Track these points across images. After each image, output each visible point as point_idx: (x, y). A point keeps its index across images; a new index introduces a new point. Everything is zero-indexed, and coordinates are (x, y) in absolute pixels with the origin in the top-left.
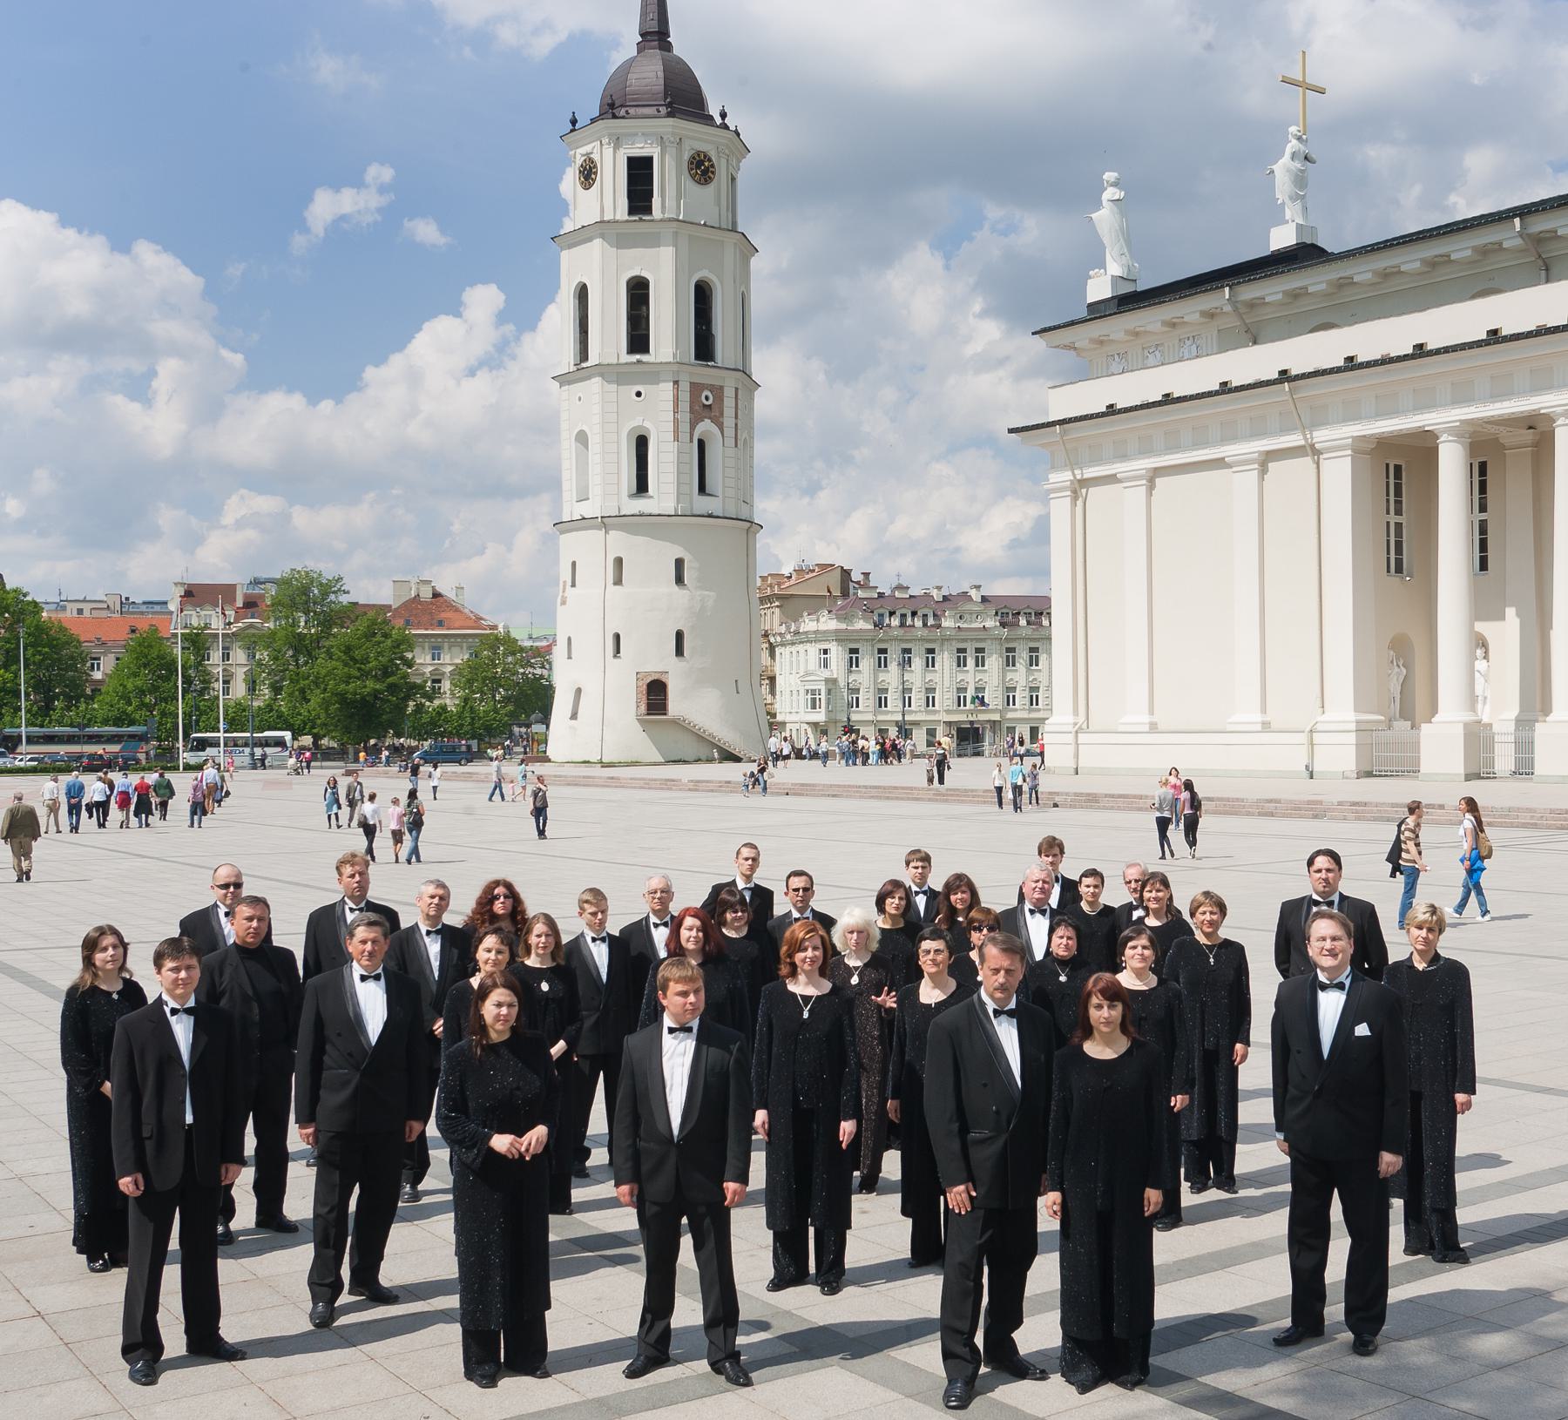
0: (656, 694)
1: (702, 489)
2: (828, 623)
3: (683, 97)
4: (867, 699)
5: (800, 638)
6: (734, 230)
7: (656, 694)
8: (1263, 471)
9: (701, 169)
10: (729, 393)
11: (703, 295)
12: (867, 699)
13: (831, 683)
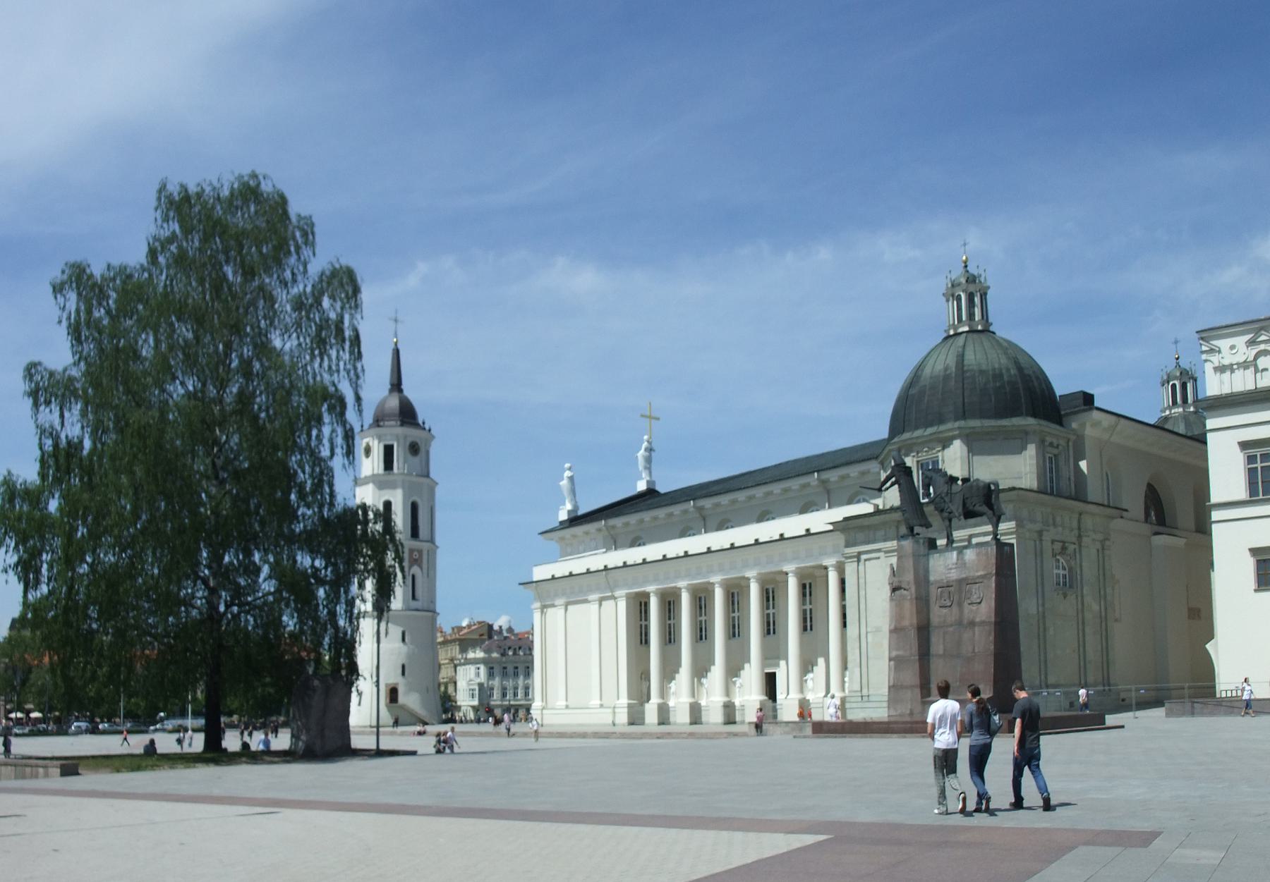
0: (393, 693)
1: (414, 597)
2: (480, 654)
3: (407, 414)
4: (497, 694)
5: (468, 662)
6: (428, 476)
7: (393, 693)
8: (600, 605)
9: (414, 449)
10: (425, 553)
11: (414, 508)
12: (497, 694)
13: (481, 685)
